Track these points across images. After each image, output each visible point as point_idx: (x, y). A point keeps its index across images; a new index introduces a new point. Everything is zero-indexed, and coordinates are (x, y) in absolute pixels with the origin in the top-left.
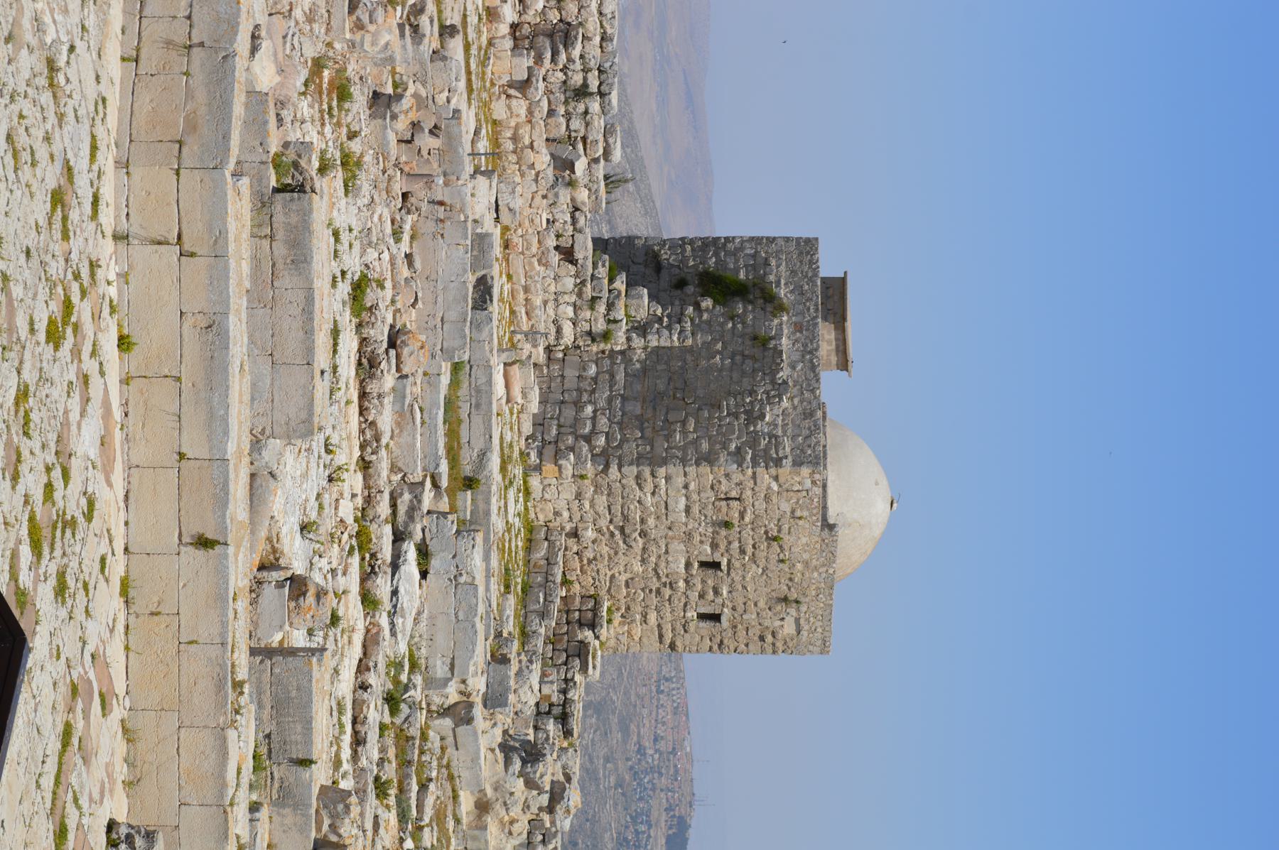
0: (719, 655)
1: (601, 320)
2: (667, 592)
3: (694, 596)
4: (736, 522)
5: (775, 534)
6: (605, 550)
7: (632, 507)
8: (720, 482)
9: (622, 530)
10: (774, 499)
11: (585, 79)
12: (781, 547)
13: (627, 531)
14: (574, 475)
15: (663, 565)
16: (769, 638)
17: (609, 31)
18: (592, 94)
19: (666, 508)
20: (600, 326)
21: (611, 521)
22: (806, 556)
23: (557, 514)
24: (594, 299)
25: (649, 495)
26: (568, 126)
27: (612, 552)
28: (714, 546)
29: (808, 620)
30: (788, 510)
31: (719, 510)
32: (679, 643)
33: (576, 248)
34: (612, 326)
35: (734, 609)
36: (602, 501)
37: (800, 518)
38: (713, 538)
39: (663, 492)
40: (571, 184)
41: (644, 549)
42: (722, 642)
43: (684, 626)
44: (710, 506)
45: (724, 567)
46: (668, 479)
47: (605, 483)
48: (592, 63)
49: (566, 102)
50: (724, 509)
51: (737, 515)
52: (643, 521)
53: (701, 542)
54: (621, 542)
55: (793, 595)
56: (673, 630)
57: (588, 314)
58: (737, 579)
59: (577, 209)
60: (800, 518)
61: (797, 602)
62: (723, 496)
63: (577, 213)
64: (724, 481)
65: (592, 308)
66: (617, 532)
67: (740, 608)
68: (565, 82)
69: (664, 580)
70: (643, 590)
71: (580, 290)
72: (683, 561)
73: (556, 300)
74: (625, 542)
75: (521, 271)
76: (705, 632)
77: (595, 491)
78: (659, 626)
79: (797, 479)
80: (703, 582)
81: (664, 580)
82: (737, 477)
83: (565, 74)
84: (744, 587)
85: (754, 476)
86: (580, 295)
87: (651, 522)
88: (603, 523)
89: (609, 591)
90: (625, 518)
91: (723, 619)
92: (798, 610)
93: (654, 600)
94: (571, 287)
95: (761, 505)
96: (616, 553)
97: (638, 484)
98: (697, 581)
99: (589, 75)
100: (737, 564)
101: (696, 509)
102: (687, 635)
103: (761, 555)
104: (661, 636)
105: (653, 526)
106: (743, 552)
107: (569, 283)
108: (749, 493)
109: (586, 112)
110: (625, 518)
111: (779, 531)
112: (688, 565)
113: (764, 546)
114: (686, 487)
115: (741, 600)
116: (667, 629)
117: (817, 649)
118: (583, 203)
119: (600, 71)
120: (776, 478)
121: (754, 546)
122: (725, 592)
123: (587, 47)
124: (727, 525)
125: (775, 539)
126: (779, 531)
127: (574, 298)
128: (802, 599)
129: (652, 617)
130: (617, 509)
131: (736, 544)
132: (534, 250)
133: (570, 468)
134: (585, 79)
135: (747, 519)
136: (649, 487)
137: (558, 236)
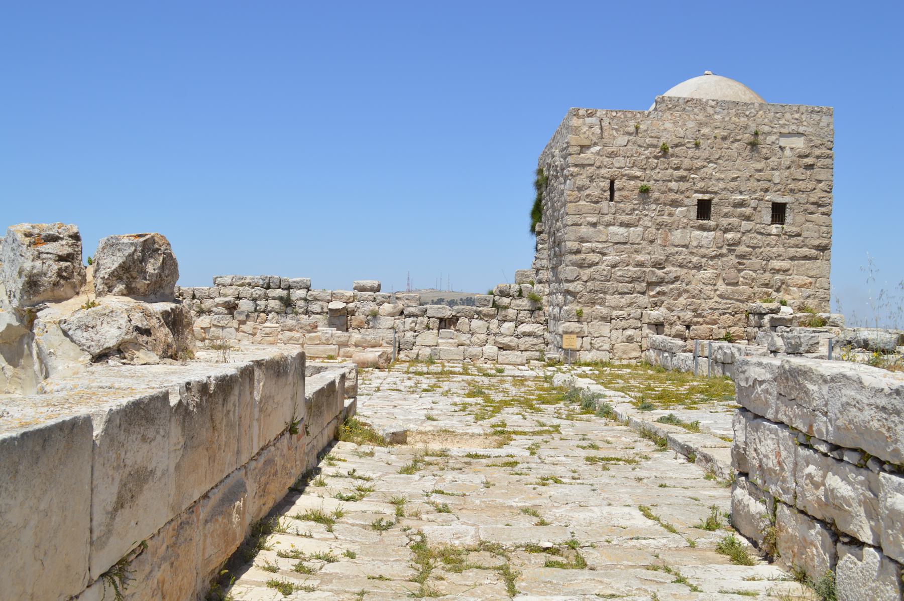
0: (834, 207)
1: (518, 302)
2: (742, 249)
3: (746, 225)
4: (640, 184)
5: (658, 150)
6: (682, 300)
7: (619, 273)
8: (588, 196)
9: (650, 285)
10: (610, 150)
11: (274, 298)
12: (676, 146)
13: (654, 279)
14: (578, 322)
15: (703, 251)
16: (809, 161)
17: (247, 281)
18: (289, 295)
19: (625, 243)
20: (525, 303)
21: (643, 293)
22: (691, 124)
23: (630, 340)
24: (495, 305)
25: (604, 258)
26: (317, 314)
27: (685, 295)
28: (675, 204)
29: (783, 126)
30: (626, 138)
31: (626, 197)
32: (817, 243)
33: (440, 315)
34: (525, 293)
35: (767, 190)
36: (611, 299)
37: (637, 128)
38: (665, 204)
39: (600, 246)
40: (375, 315)
41: (681, 266)
42: (813, 204)
43: (790, 236)
44: (621, 205)
45: (706, 197)
46: (582, 240)
47: (588, 296)
48: (258, 292)
49: (297, 313)
50: (625, 193)
51: (632, 183)
52: (640, 265)
53: (670, 215)
54: (671, 286)
55: (748, 137)
56: (797, 246)
57: (510, 311)
58: (721, 185)
59: (402, 313)
60: (637, 128)
61: (756, 134)
62: (608, 194)
63: (405, 312)
64: (587, 192)
65: (506, 308)
66: (658, 289)
67: (766, 185)
68: (278, 313)
69: (724, 251)
70: (740, 271)
71: (485, 315)
72: (697, 233)
73: (495, 335)
74: (673, 283)
75: (321, 347)
76: (800, 218)
77: (600, 304)
78: (792, 259)
79: (585, 129)
80: (726, 215)
81: (724, 251)
82: (581, 180)
83: (270, 312)
84: (734, 179)
85: (583, 166)
86: (492, 317)
87: (640, 258)
88: (643, 300)
89: (742, 302)
90: (633, 280)
91: (780, 200)
92: (769, 134)
93: (756, 262)
94: (481, 323)
95: (619, 162)
96: (688, 292)
97: (590, 266)
98: (724, 222)
99: (270, 295)
100: (700, 185)
101: (624, 218)
102: (805, 234)
103: (687, 163)
104: (806, 258)
105: (648, 257)
106: (682, 179)
107: (476, 323)
108: (603, 171)
109: (305, 300)
110: (633, 280)
111: (655, 146)
112: (703, 228)
113: (675, 161)
114: (594, 225)
115: (753, 184)
116: (792, 251)
117: (825, 120)
118: (395, 308)
119: (268, 287)
120: (583, 148)
121: (678, 169)
122: (742, 197)
123: (244, 295)
124: (645, 191)
125: (665, 150)
126: (655, 146)
127: (494, 323)
128: (753, 128)
129: (776, 264)
130: (621, 287)
131: (673, 185)
132: (296, 335)
133: (567, 324)
134: (274, 298)
135: (638, 174)
136: (595, 258)
137: (428, 328)
